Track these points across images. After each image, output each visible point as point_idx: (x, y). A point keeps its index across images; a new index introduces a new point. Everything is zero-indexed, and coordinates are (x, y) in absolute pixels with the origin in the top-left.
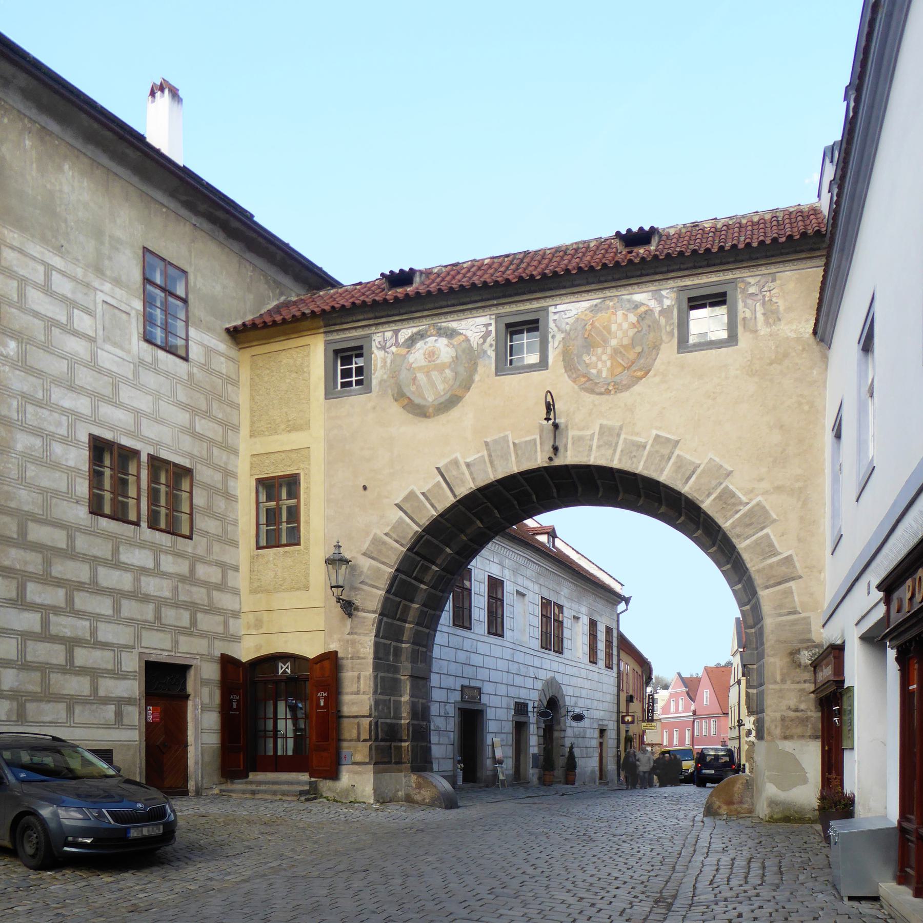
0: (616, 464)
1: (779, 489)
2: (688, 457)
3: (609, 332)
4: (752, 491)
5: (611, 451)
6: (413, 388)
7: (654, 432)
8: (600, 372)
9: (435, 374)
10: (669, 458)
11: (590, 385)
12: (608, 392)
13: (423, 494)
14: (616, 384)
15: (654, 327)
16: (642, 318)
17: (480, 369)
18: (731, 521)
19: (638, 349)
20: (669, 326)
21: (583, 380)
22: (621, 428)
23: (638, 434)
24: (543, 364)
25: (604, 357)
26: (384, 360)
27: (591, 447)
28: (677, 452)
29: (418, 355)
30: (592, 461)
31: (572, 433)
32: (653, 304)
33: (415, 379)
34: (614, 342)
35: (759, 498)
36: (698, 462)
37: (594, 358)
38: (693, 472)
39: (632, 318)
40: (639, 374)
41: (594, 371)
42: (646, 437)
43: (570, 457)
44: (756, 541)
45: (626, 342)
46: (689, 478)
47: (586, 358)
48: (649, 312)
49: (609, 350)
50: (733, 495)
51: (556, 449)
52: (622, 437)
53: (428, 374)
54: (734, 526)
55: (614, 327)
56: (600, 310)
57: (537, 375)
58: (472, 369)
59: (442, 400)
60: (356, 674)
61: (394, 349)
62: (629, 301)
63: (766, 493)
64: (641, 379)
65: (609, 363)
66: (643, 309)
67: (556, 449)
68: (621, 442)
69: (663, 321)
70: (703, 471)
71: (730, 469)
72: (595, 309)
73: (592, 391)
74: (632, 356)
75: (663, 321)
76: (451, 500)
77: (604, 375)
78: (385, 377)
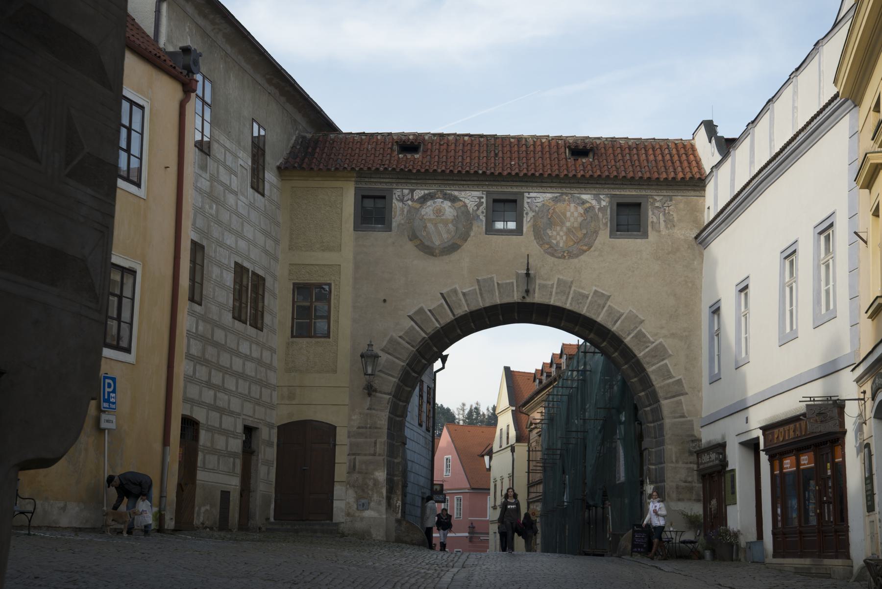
0: (568, 306)
1: (673, 335)
2: (616, 307)
3: (565, 216)
4: (656, 335)
5: (565, 298)
6: (424, 234)
7: (594, 288)
8: (558, 243)
9: (440, 226)
10: (604, 307)
11: (552, 251)
12: (563, 257)
13: (430, 311)
14: (569, 252)
15: (595, 218)
16: (587, 210)
17: (475, 228)
18: (643, 353)
19: (584, 231)
20: (605, 220)
21: (547, 246)
22: (572, 282)
23: (582, 288)
24: (519, 231)
25: (561, 233)
26: (402, 210)
27: (551, 293)
28: (609, 303)
29: (428, 210)
30: (552, 303)
31: (538, 282)
32: (594, 202)
33: (425, 227)
34: (568, 224)
35: (661, 340)
36: (622, 311)
37: (555, 233)
38: (619, 318)
39: (581, 210)
40: (585, 248)
41: (554, 242)
42: (589, 291)
43: (538, 298)
44: (659, 367)
45: (576, 225)
46: (616, 321)
47: (549, 232)
48: (592, 208)
49: (565, 229)
50: (645, 336)
51: (527, 291)
52: (573, 288)
53: (435, 225)
54: (645, 356)
55: (568, 214)
56: (559, 201)
57: (515, 239)
58: (469, 228)
59: (446, 245)
60: (373, 440)
61: (410, 202)
62: (579, 198)
63: (665, 336)
64: (586, 251)
65: (564, 238)
66: (588, 205)
67: (527, 291)
68: (572, 292)
69: (600, 215)
70: (626, 318)
71: (643, 318)
72: (556, 200)
73: (553, 255)
74: (580, 235)
75: (600, 215)
76: (451, 317)
77: (561, 245)
78: (403, 222)
